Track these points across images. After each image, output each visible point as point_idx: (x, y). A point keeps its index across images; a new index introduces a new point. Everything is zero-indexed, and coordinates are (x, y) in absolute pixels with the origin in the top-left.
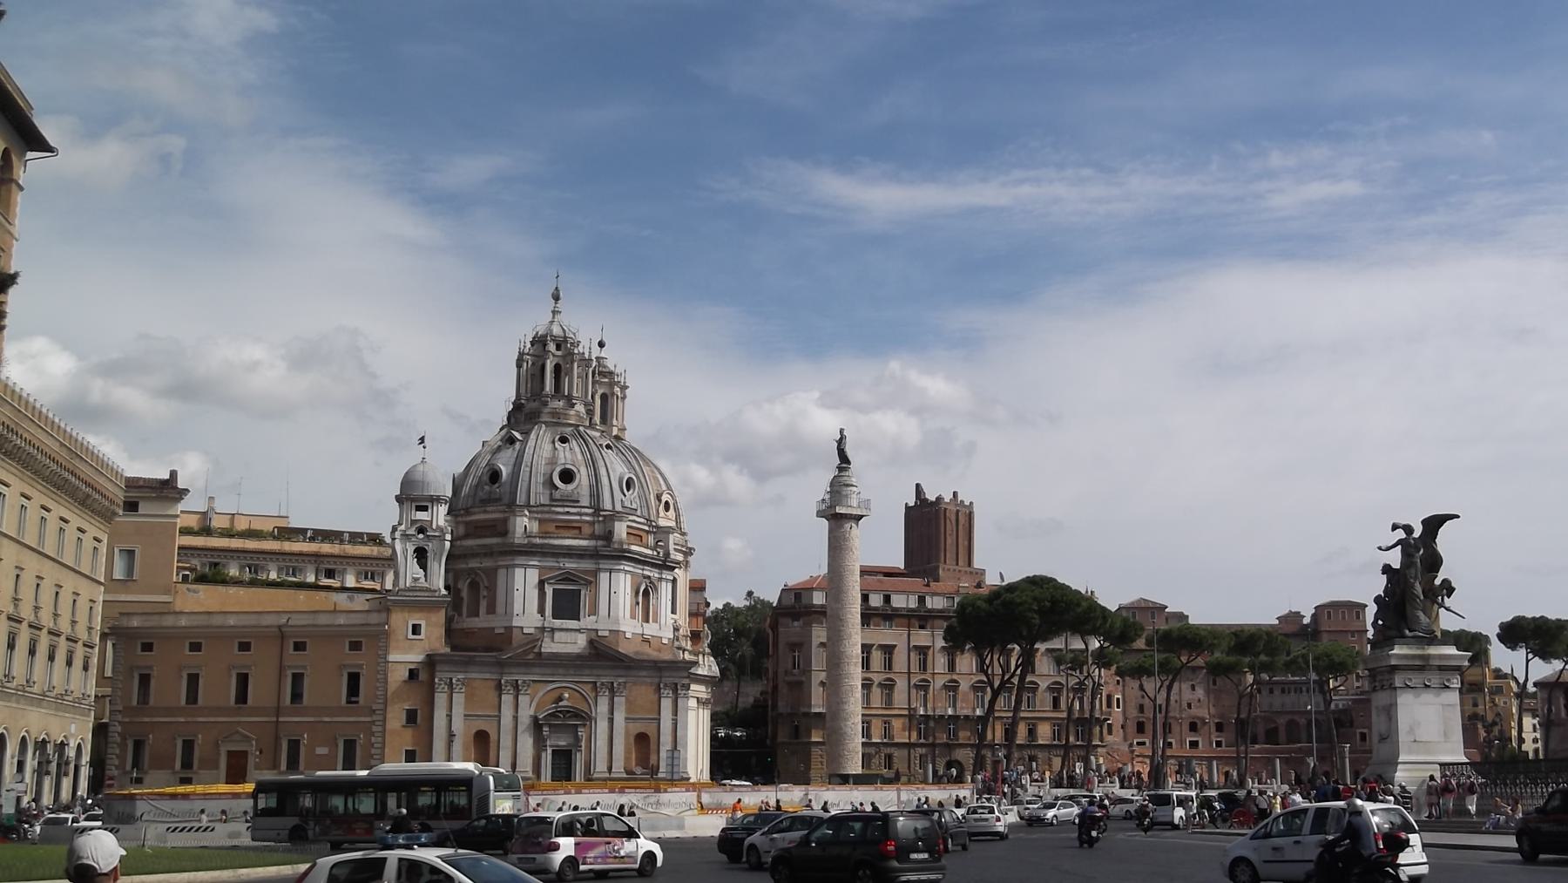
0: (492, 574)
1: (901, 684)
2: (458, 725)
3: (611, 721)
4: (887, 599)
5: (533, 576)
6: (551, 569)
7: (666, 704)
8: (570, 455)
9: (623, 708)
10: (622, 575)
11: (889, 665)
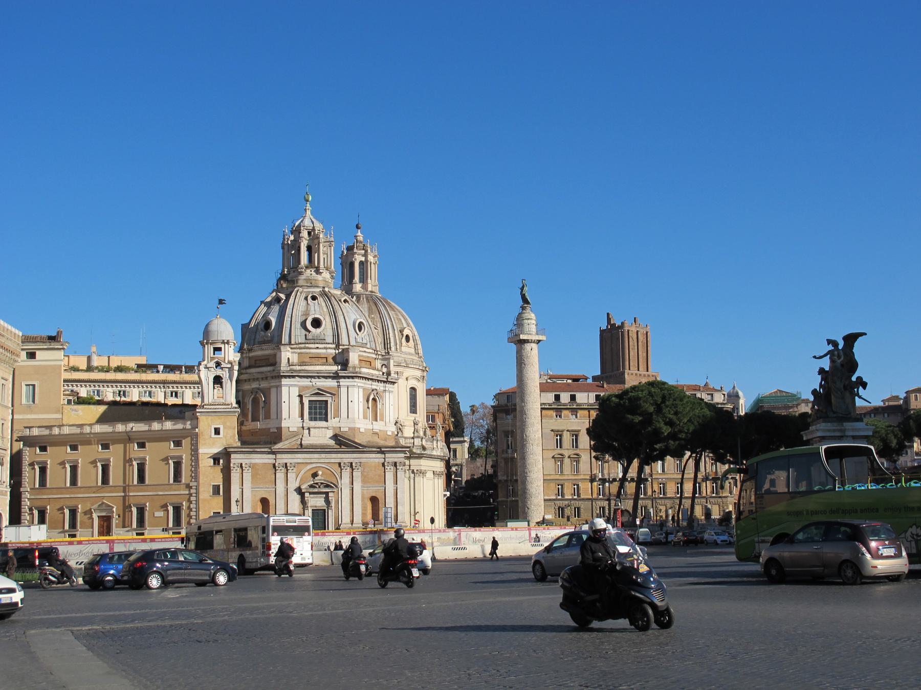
0: (266, 392)
4: (573, 398)
5: (295, 392)
6: (307, 388)
8: (318, 310)
9: (359, 480)
10: (356, 389)
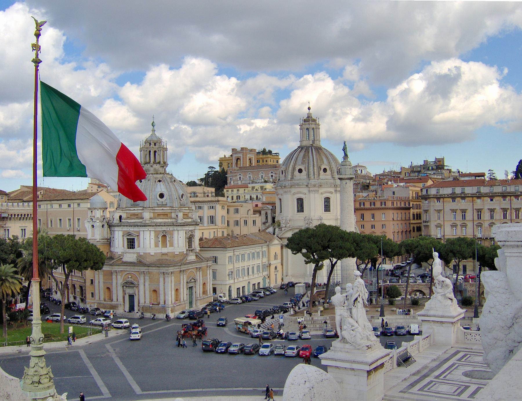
1: (470, 225)
2: (101, 284)
3: (145, 285)
5: (121, 233)
7: (161, 279)
9: (148, 281)
11: (464, 217)
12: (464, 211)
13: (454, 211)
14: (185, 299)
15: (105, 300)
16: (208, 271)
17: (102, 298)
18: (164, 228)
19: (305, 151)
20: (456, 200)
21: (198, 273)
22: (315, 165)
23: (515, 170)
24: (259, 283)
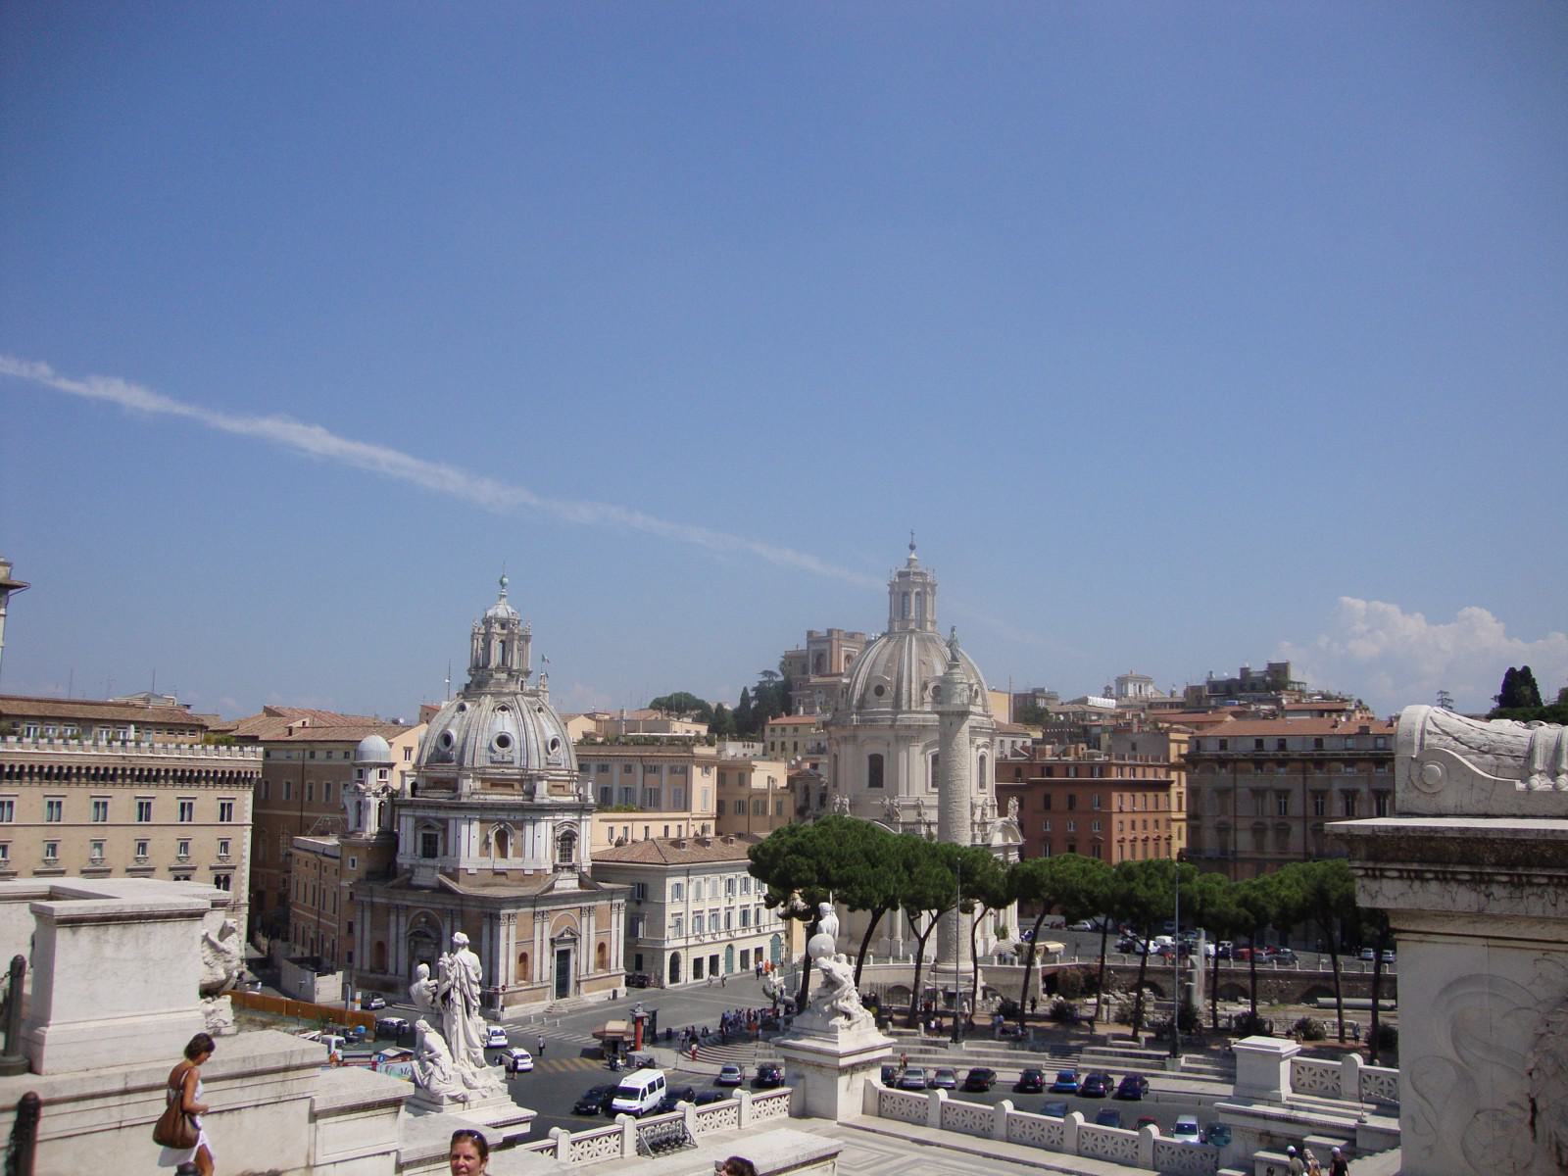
1: (1297, 829)
2: (367, 936)
5: (411, 822)
11: (1283, 809)
12: (1283, 794)
13: (1258, 793)
14: (546, 976)
15: (372, 971)
16: (614, 918)
17: (367, 967)
18: (503, 816)
19: (895, 646)
20: (1265, 768)
21: (585, 920)
22: (914, 680)
23: (1500, 693)
24: (759, 951)
